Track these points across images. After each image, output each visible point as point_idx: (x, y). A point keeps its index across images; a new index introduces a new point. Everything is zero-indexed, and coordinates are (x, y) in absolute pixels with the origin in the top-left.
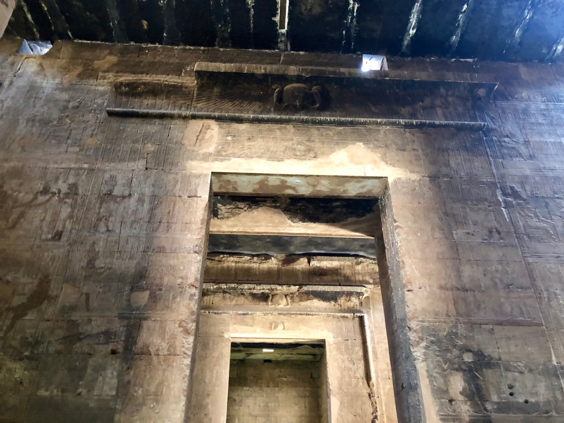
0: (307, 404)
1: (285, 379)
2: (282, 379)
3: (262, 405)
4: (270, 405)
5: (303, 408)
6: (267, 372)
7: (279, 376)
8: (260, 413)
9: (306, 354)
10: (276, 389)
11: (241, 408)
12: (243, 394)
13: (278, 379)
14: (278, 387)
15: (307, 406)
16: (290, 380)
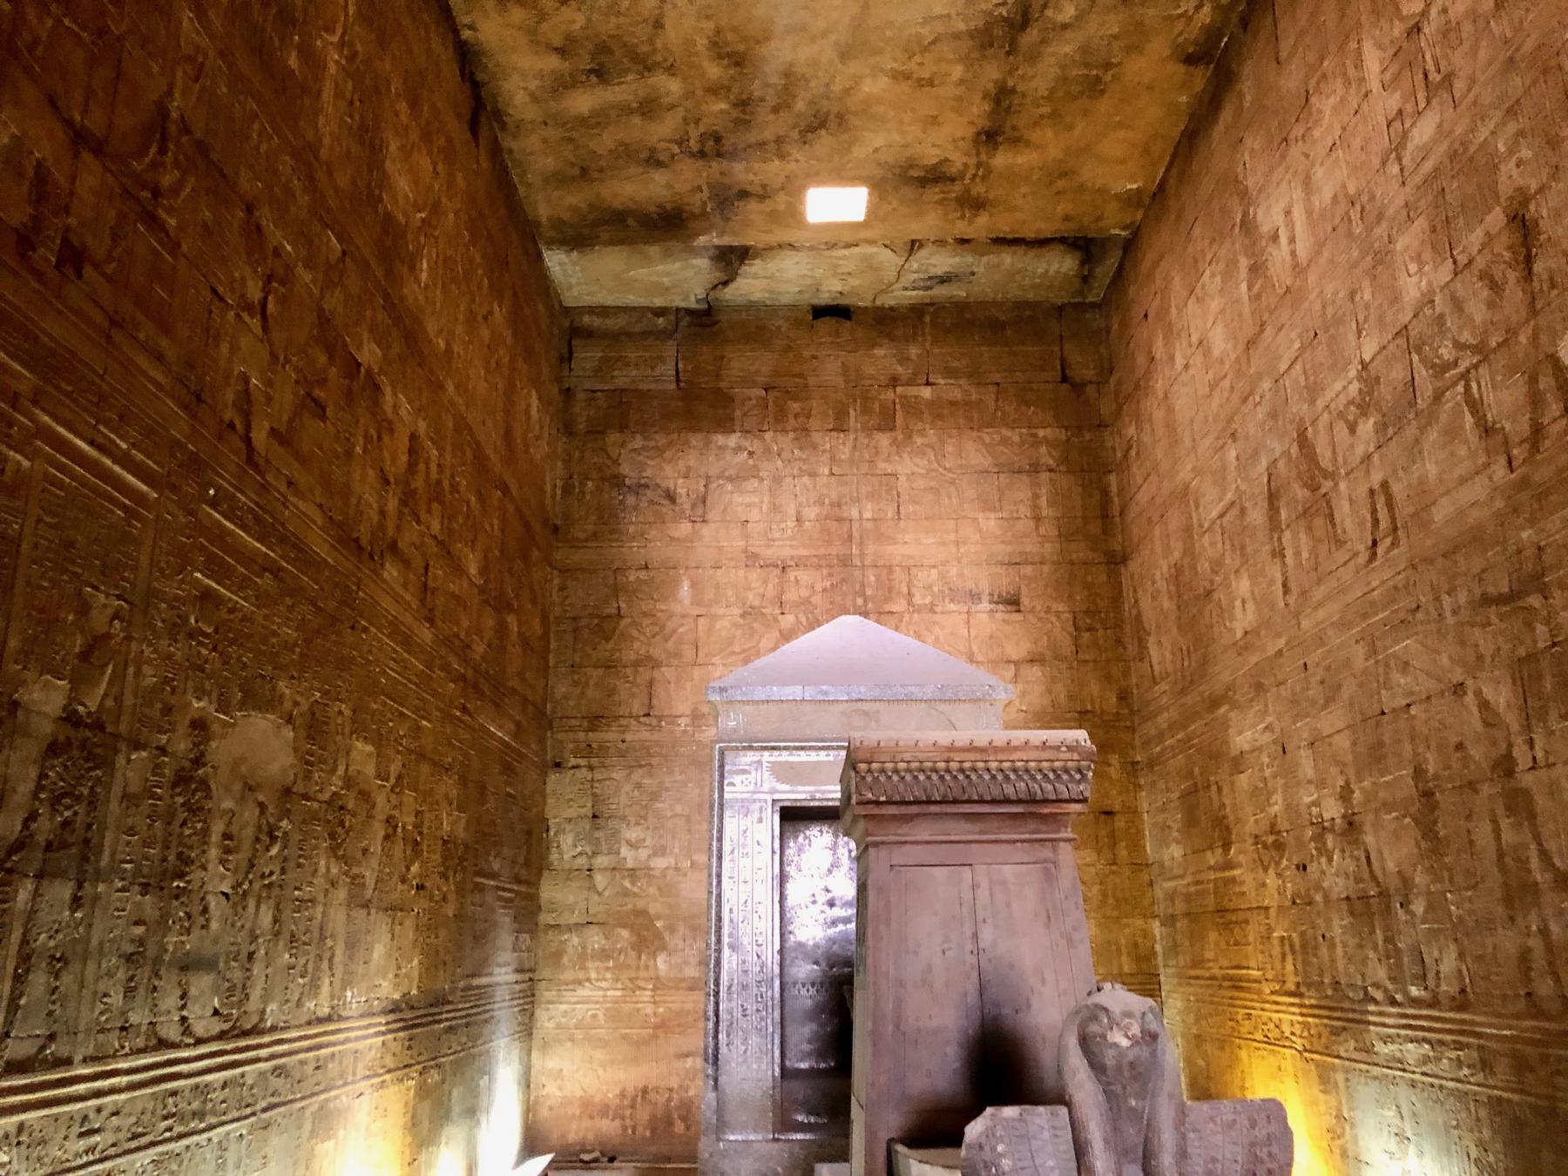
0: (1043, 502)
1: (927, 393)
2: (912, 391)
3: (811, 513)
4: (855, 513)
5: (1025, 525)
6: (830, 363)
7: (894, 382)
8: (803, 552)
9: (1042, 243)
10: (883, 440)
11: (706, 531)
12: (713, 466)
13: (889, 395)
14: (893, 429)
15: (1046, 511)
16: (957, 394)
